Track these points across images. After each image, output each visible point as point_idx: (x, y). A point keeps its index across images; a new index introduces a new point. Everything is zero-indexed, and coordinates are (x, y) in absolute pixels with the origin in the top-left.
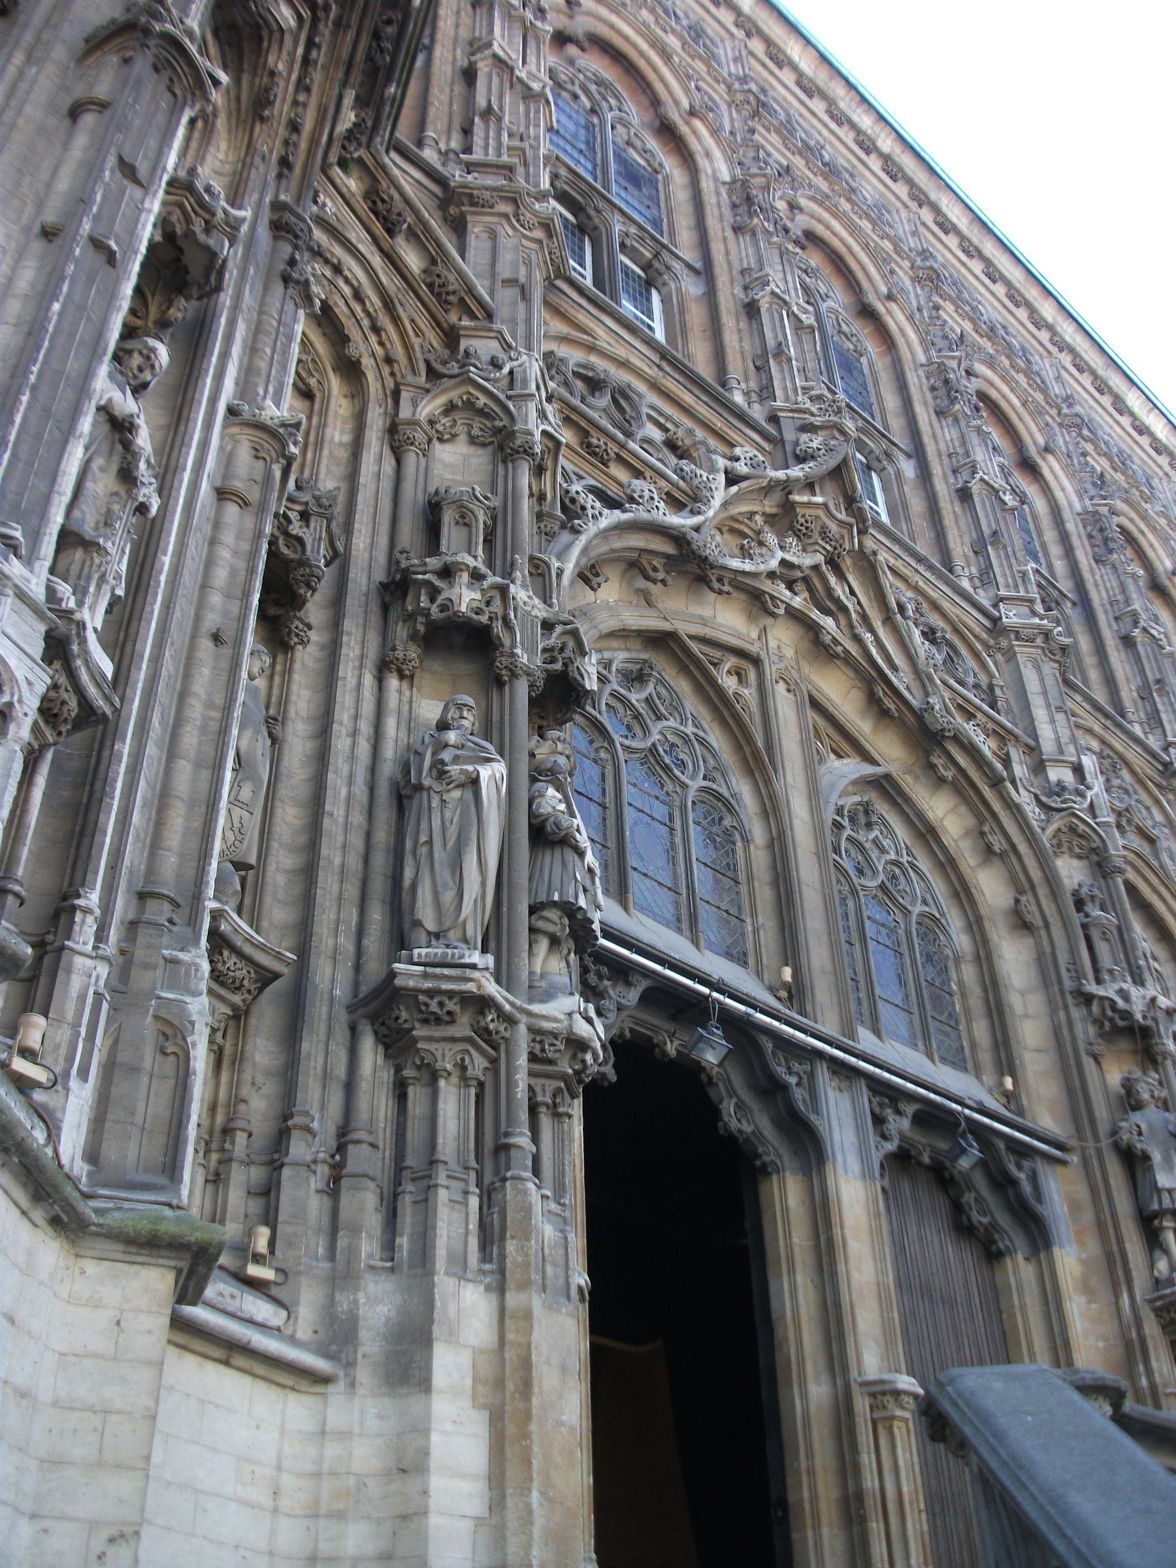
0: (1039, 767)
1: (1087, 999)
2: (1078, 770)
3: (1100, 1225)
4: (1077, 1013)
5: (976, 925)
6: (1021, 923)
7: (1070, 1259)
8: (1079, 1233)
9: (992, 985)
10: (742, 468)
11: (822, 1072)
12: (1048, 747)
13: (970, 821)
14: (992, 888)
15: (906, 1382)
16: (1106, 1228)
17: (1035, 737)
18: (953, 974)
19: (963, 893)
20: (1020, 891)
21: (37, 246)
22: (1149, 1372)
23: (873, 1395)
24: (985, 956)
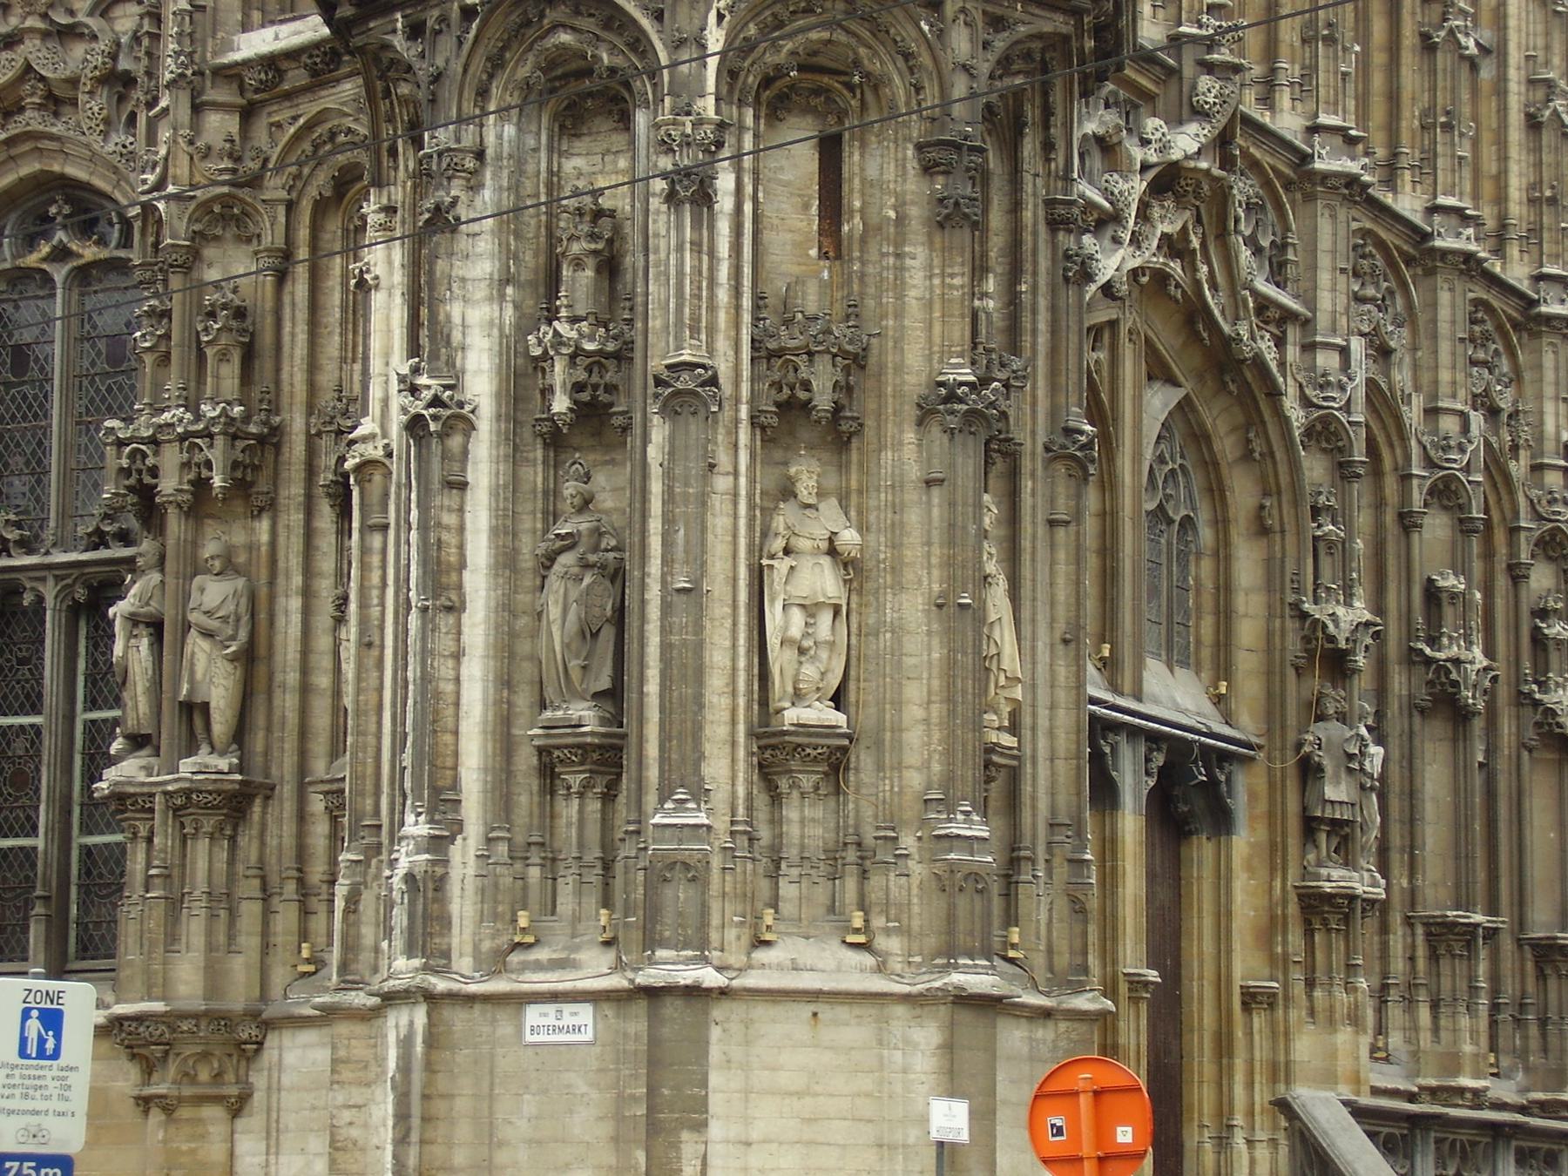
0: (1309, 348)
1: (1304, 616)
2: (1344, 351)
3: (1271, 815)
4: (1291, 625)
5: (1222, 523)
6: (1262, 530)
7: (1244, 841)
8: (1252, 818)
9: (1225, 587)
10: (1154, 159)
11: (1122, 740)
12: (1323, 321)
13: (1241, 419)
14: (1243, 493)
15: (1153, 975)
16: (1274, 818)
17: (1312, 304)
18: (1192, 568)
19: (1217, 492)
20: (1266, 493)
21: (1060, 647)
22: (1285, 943)
23: (1131, 983)
24: (1223, 555)
